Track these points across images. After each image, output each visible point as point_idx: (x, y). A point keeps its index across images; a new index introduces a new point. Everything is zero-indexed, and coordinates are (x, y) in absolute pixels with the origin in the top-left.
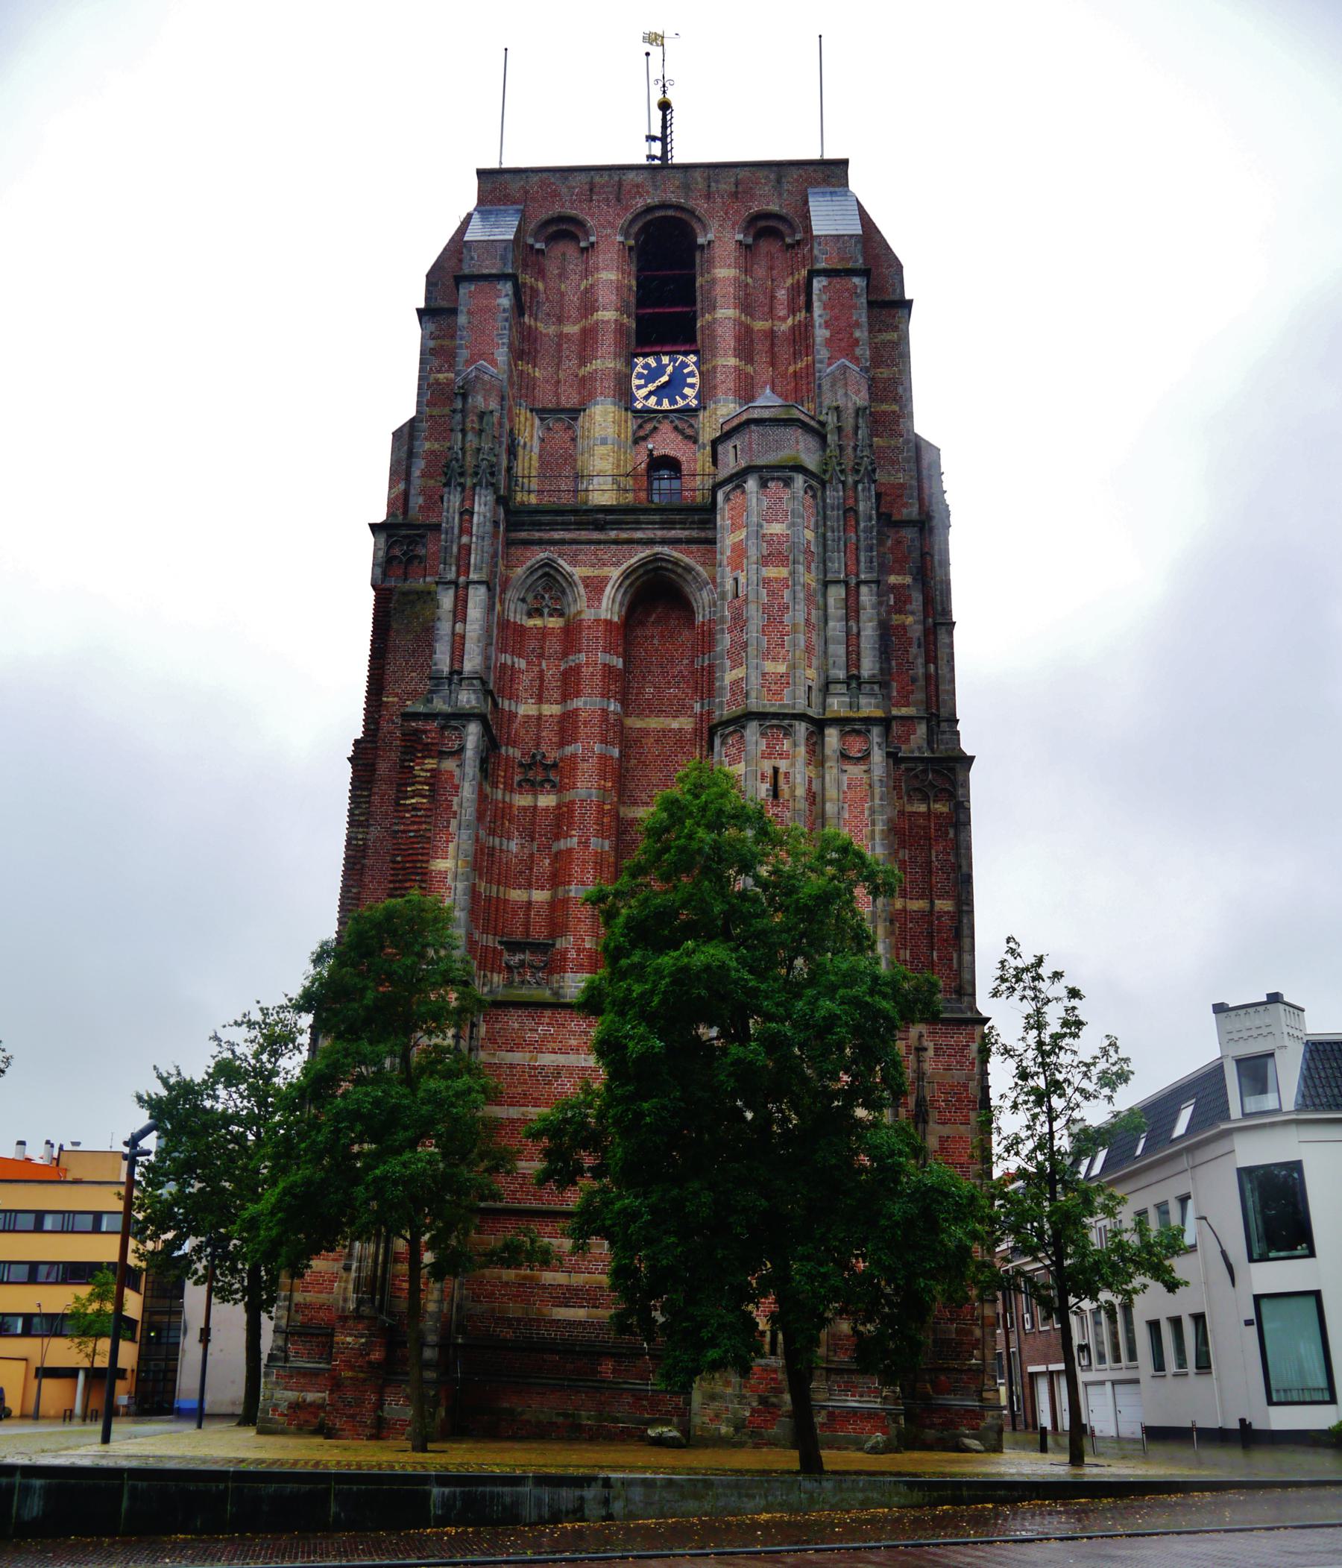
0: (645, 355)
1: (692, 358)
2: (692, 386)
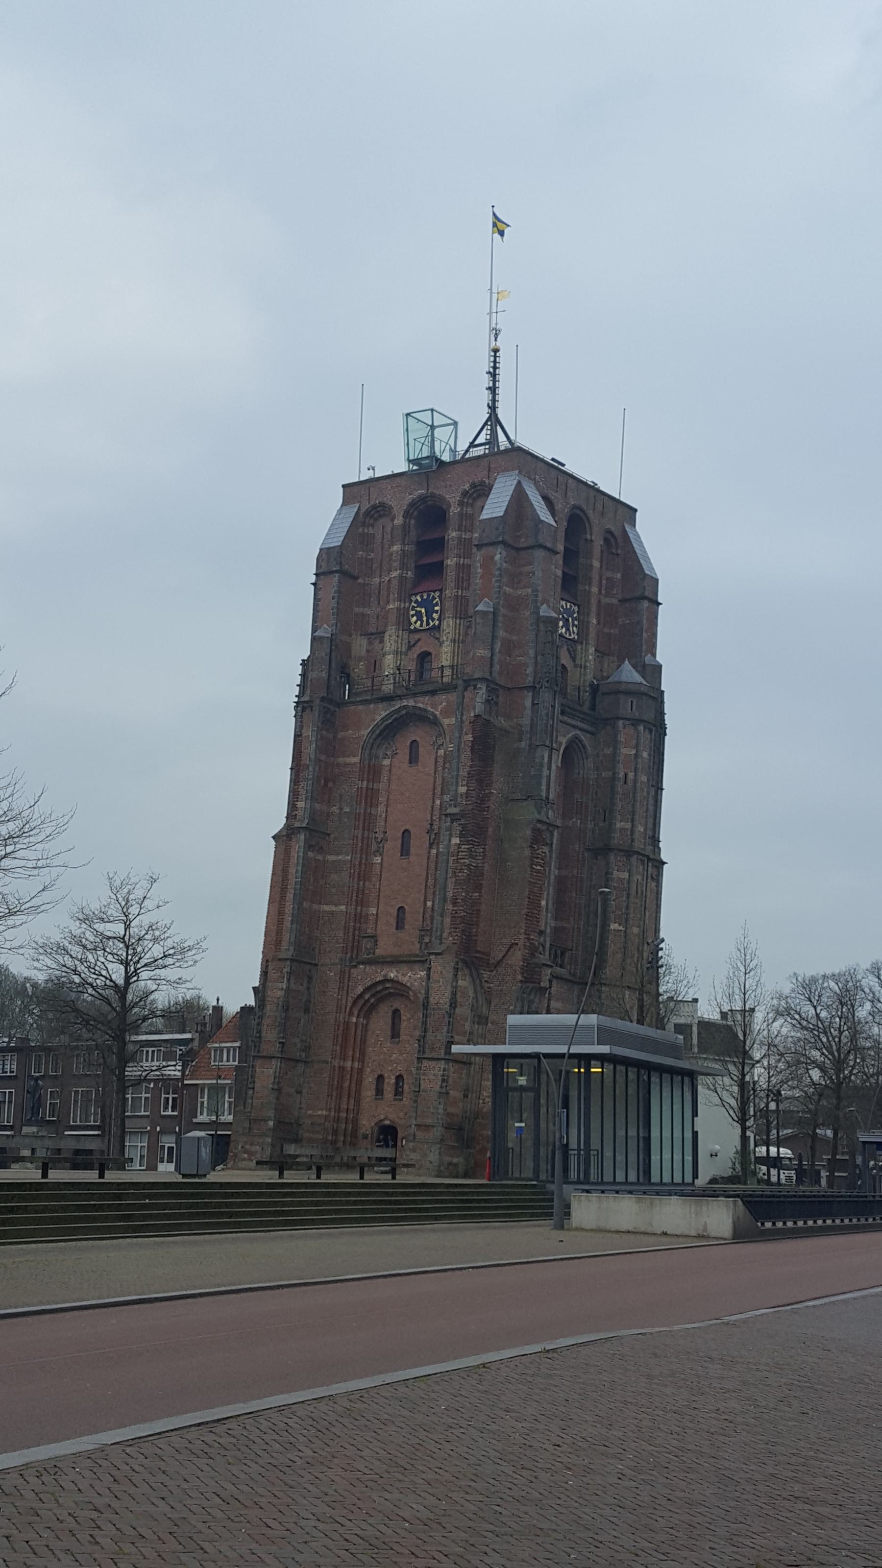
0: (416, 595)
1: (437, 594)
2: (437, 612)
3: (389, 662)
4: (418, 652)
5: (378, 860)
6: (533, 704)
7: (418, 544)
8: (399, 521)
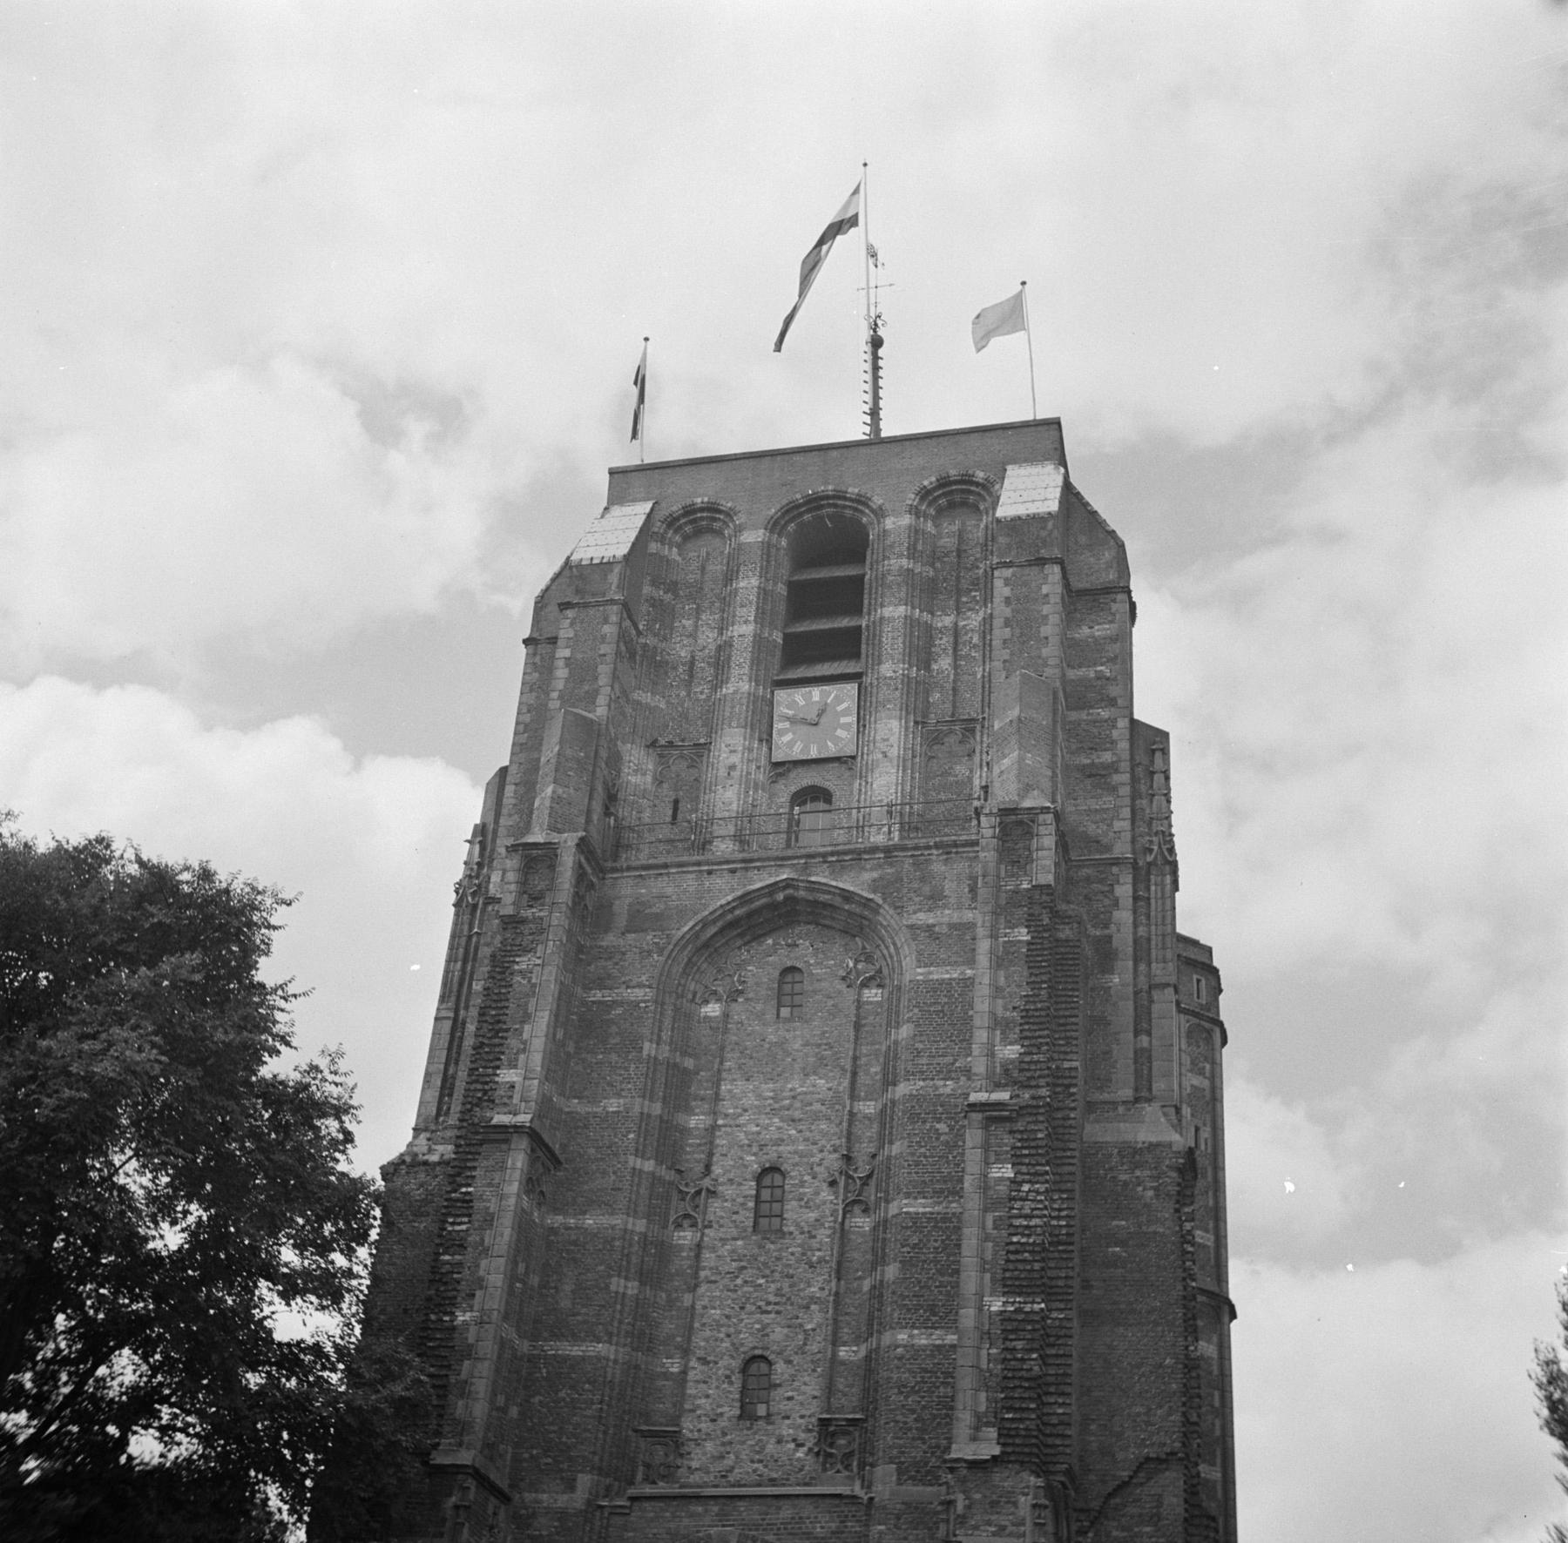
3: (727, 798)
4: (793, 789)
5: (686, 1237)
6: (1136, 898)
7: (791, 585)
8: (753, 536)
